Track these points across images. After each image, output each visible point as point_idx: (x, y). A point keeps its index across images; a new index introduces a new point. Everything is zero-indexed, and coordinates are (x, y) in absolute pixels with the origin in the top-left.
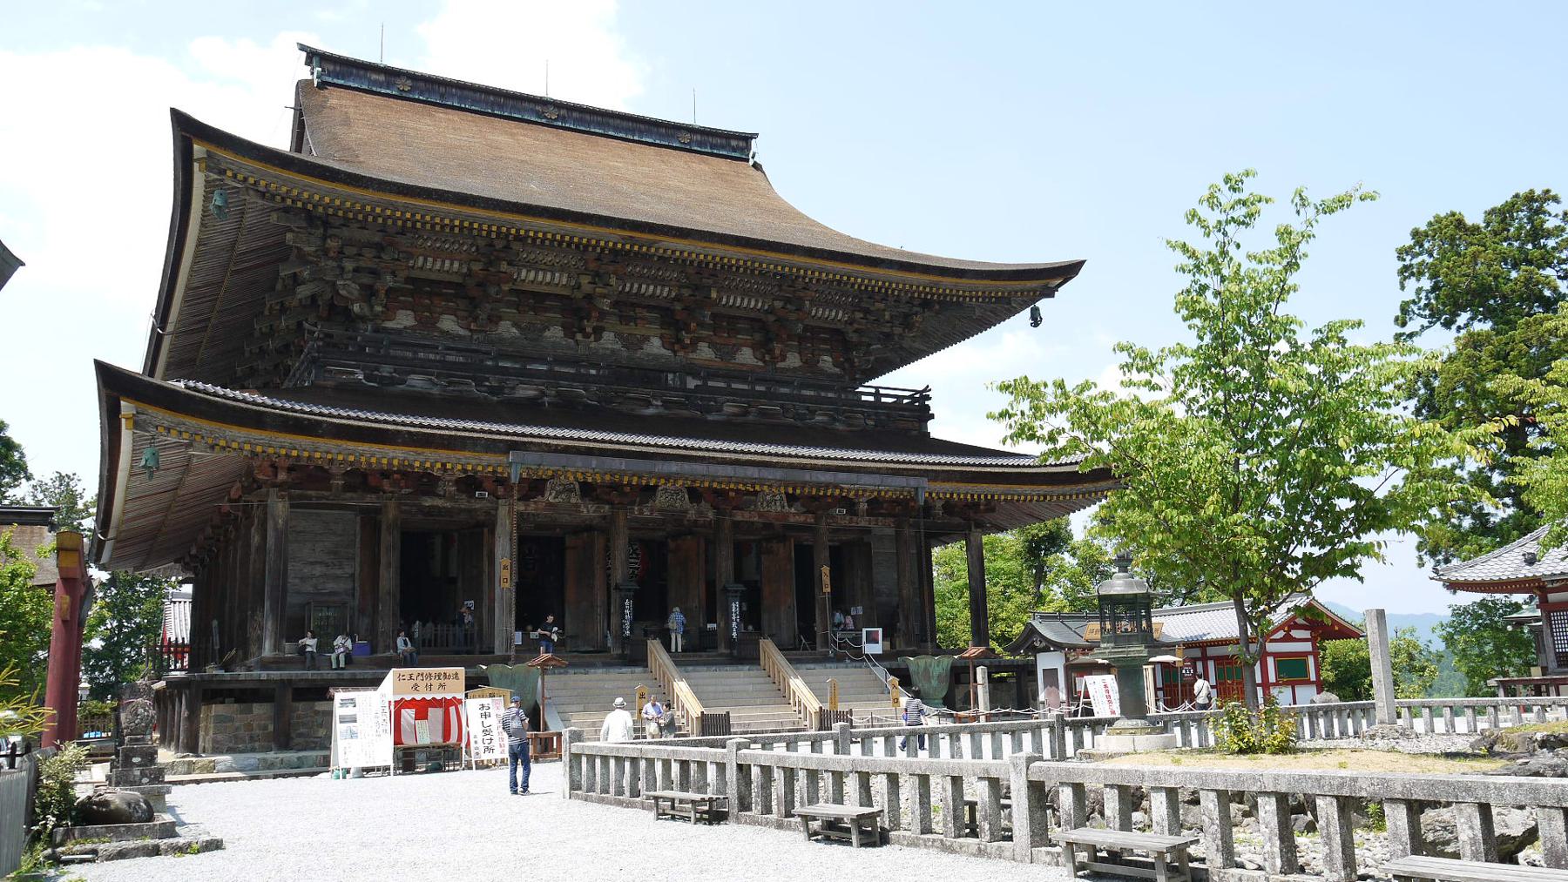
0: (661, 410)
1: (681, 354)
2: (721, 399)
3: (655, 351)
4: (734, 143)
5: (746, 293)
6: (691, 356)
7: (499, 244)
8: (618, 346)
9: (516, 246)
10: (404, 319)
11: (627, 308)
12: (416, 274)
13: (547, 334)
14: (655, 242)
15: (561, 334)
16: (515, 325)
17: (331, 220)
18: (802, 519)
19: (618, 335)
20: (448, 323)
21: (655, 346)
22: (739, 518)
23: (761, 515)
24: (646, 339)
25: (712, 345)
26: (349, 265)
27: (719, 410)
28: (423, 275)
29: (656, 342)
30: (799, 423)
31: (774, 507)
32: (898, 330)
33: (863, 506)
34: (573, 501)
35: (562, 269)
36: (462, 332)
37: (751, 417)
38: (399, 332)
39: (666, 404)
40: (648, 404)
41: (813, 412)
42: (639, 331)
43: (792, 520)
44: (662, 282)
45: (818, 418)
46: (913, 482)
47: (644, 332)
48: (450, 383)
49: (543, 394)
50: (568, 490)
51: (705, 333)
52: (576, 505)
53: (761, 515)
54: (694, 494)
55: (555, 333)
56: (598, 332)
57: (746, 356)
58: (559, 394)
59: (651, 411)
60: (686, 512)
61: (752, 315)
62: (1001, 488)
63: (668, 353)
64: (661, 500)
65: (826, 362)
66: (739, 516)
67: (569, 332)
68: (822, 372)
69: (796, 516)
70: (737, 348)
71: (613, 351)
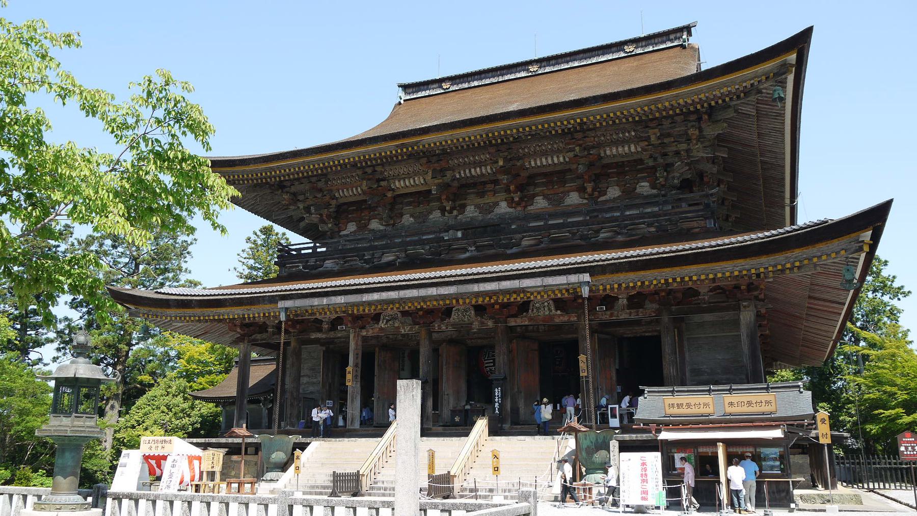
0: (475, 253)
1: (519, 209)
2: (519, 236)
3: (503, 211)
4: (672, 37)
5: (545, 154)
6: (529, 208)
7: (369, 170)
8: (476, 214)
9: (379, 169)
10: (352, 227)
11: (478, 186)
12: (341, 201)
13: (431, 217)
14: (417, 142)
15: (440, 215)
16: (412, 216)
17: (285, 184)
18: (566, 318)
19: (477, 206)
20: (375, 225)
21: (503, 208)
22: (513, 324)
23: (531, 319)
24: (496, 204)
25: (546, 197)
26: (301, 206)
27: (519, 245)
28: (346, 200)
29: (504, 204)
30: (583, 243)
31: (544, 311)
32: (684, 146)
33: (623, 301)
34: (396, 325)
35: (416, 174)
36: (382, 228)
37: (542, 245)
38: (347, 235)
39: (478, 248)
40: (465, 250)
41: (598, 232)
42: (489, 199)
43: (557, 320)
44: (480, 164)
45: (602, 235)
46: (573, 278)
47: (493, 199)
48: (345, 262)
49: (398, 258)
50: (394, 318)
51: (538, 189)
52: (398, 328)
53: (531, 319)
54: (480, 309)
55: (436, 215)
56: (463, 207)
57: (574, 198)
58: (407, 255)
59: (468, 254)
60: (471, 324)
61: (558, 168)
62: (694, 268)
63: (511, 210)
64: (454, 317)
65: (644, 188)
66: (512, 322)
67: (443, 210)
68: (640, 196)
69: (560, 318)
70: (566, 193)
71: (472, 218)
